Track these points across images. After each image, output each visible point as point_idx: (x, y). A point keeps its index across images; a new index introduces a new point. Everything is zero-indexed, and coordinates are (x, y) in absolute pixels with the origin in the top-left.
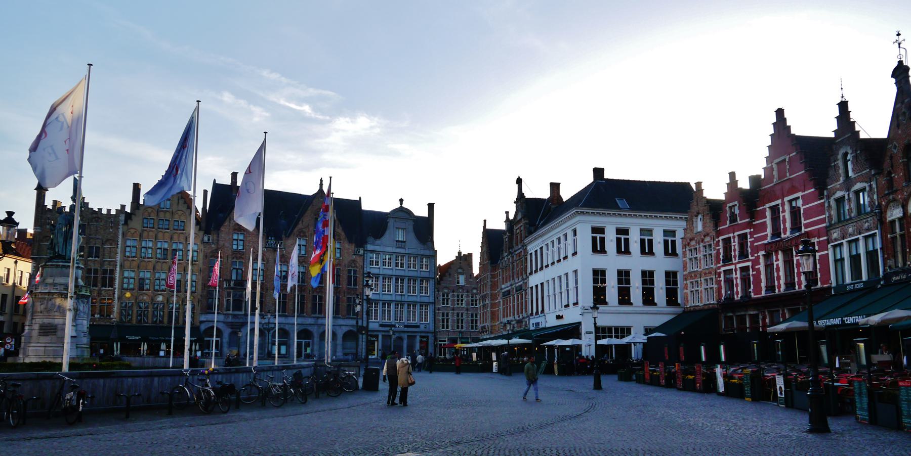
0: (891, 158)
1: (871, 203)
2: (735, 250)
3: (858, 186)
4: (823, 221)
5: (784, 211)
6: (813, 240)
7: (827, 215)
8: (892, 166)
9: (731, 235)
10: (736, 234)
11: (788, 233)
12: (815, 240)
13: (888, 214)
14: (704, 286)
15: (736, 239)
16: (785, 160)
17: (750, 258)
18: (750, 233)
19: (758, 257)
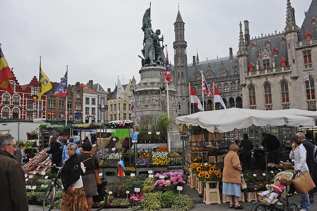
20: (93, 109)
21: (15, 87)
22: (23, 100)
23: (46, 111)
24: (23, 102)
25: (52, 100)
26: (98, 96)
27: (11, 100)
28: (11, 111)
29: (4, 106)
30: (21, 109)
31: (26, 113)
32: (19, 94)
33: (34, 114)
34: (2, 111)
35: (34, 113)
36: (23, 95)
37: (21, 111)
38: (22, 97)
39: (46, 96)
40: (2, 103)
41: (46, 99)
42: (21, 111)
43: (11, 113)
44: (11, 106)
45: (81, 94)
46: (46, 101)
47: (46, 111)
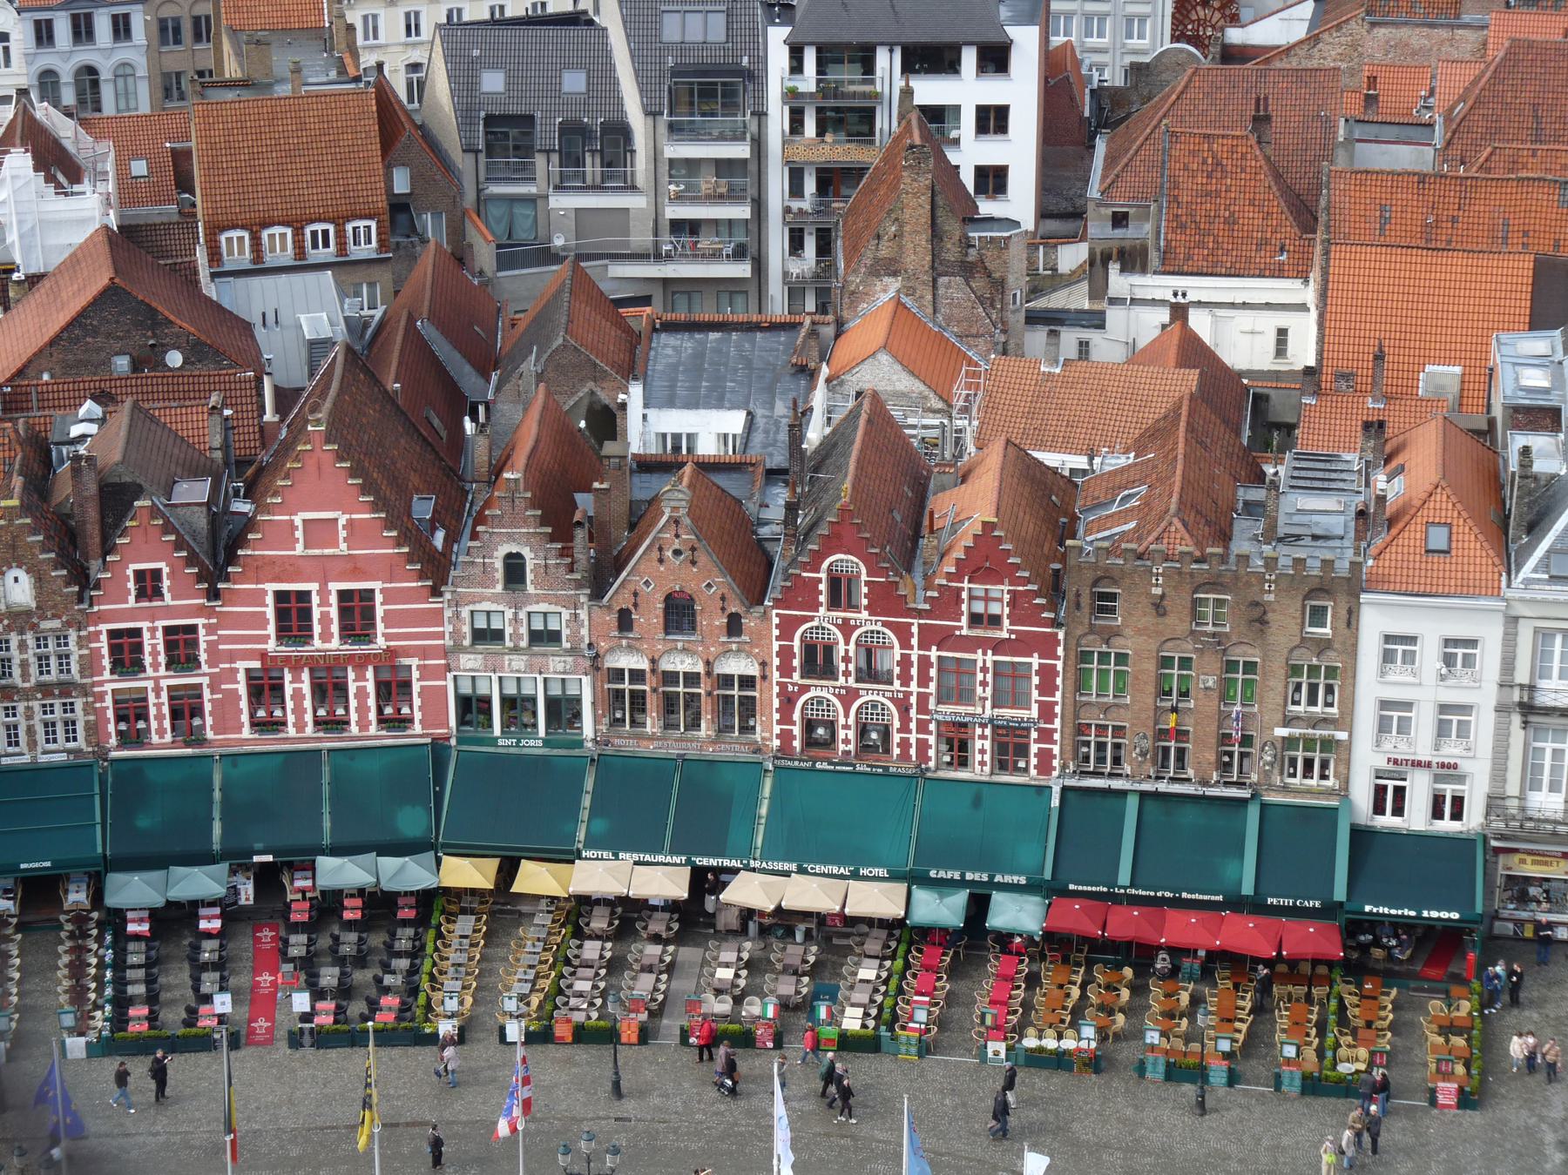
0: (635, 594)
1: (575, 637)
2: (154, 653)
3: (543, 607)
4: (441, 636)
5: (324, 602)
6: (406, 661)
7: (449, 628)
8: (635, 605)
9: (144, 625)
10: (160, 624)
11: (335, 643)
12: (414, 662)
13: (608, 657)
14: (38, 716)
15: (160, 634)
16: (336, 520)
17: (205, 668)
18: (204, 626)
19: (236, 670)
20: (1451, 718)
21: (865, 590)
22: (914, 659)
23: (1057, 723)
24: (914, 671)
25: (1104, 657)
26: (1513, 621)
27: (846, 659)
28: (847, 716)
29: (804, 689)
30: (903, 706)
31: (932, 727)
32: (885, 624)
33: (983, 737)
34: (797, 716)
35: (979, 731)
36: (915, 629)
37: (905, 720)
38: (906, 644)
39: (1061, 636)
40: (796, 676)
41: (1060, 651)
42: (905, 720)
43: (846, 727)
44: (843, 692)
45: (1343, 613)
46: (1060, 665)
47: (1058, 722)
